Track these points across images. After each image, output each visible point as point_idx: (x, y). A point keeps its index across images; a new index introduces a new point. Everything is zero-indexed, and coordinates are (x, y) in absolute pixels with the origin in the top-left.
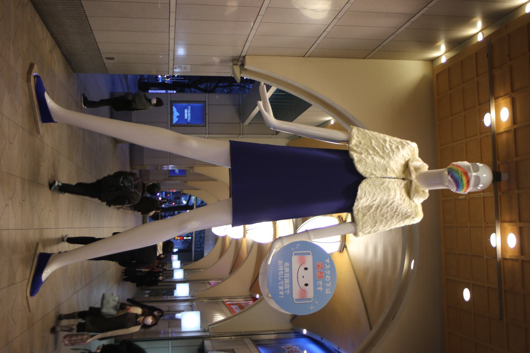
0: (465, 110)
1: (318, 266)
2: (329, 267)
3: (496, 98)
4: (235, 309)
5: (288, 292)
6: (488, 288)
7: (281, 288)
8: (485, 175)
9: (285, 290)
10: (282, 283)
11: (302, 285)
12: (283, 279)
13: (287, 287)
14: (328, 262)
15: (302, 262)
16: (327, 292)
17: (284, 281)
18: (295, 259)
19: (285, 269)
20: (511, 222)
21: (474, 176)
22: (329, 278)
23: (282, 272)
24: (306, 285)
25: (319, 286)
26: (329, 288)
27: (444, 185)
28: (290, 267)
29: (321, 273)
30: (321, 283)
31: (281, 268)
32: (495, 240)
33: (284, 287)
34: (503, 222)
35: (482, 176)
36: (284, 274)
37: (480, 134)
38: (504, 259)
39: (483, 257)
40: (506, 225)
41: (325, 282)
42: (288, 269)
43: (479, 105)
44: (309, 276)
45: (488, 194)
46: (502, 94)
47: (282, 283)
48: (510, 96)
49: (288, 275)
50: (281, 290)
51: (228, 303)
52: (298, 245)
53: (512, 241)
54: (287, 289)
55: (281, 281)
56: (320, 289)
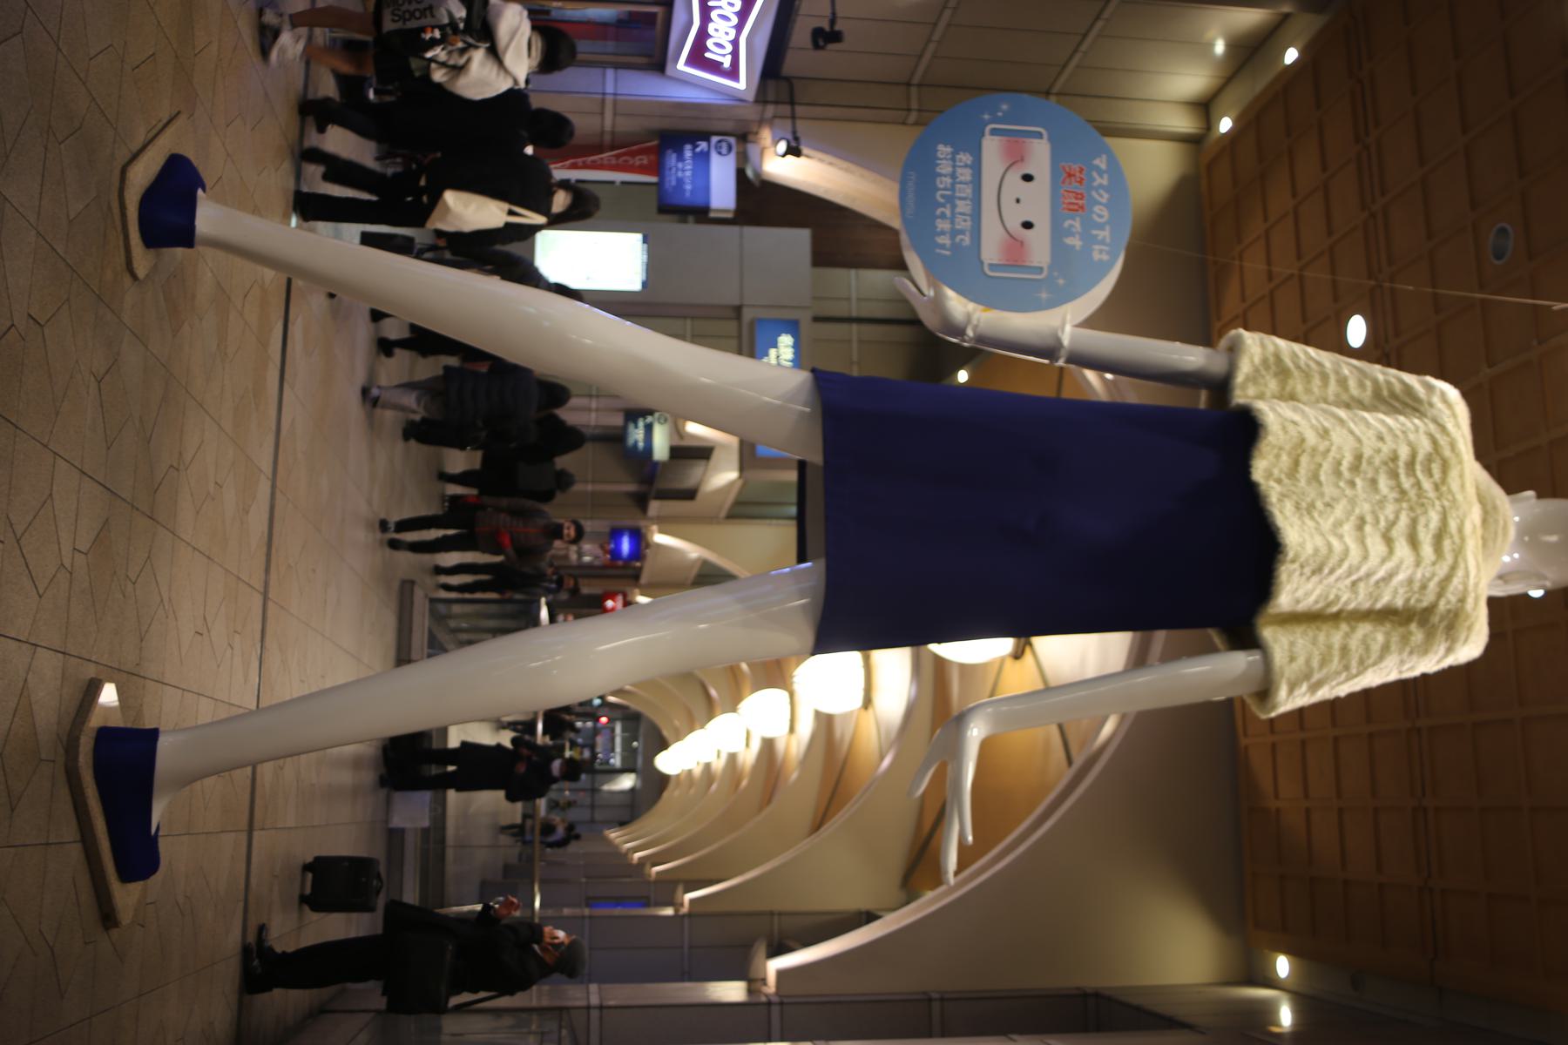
2: (1105, 182)
5: (967, 240)
7: (942, 225)
9: (954, 233)
10: (948, 212)
11: (1014, 225)
12: (951, 200)
13: (964, 224)
14: (1103, 166)
15: (1015, 157)
16: (1096, 256)
19: (959, 171)
22: (1105, 213)
23: (949, 180)
24: (1028, 225)
25: (1071, 234)
26: (1103, 242)
28: (977, 168)
29: (1079, 196)
30: (1077, 225)
31: (944, 168)
36: (953, 185)
41: (1089, 224)
44: (1037, 201)
47: (948, 212)
50: (943, 233)
54: (962, 232)
55: (943, 205)
56: (1075, 242)
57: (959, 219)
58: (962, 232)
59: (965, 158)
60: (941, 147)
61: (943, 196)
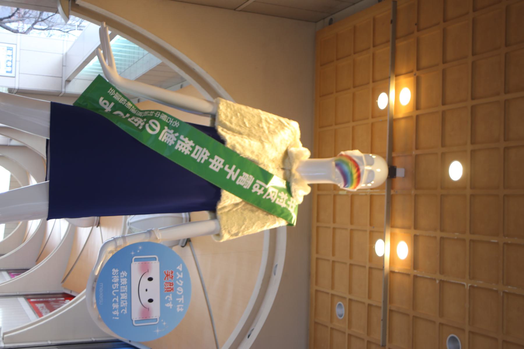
0: (354, 87)
3: (397, 76)
4: (40, 309)
6: (369, 305)
7: (115, 306)
8: (378, 170)
9: (120, 309)
11: (145, 301)
12: (118, 294)
13: (124, 304)
15: (145, 270)
17: (120, 297)
18: (135, 267)
19: (122, 280)
20: (402, 227)
21: (367, 170)
23: (117, 285)
27: (330, 179)
31: (116, 279)
32: (381, 248)
33: (119, 304)
34: (392, 227)
35: (375, 170)
36: (119, 287)
37: (373, 117)
38: (392, 272)
39: (365, 267)
40: (397, 231)
42: (125, 279)
43: (373, 82)
45: (376, 192)
46: (404, 71)
48: (415, 75)
49: (126, 288)
50: (115, 309)
51: (32, 300)
52: (140, 248)
53: (403, 250)
54: (124, 308)
55: (116, 297)
57: (122, 302)
58: (124, 308)
59: (124, 274)
60: (114, 270)
61: (115, 293)
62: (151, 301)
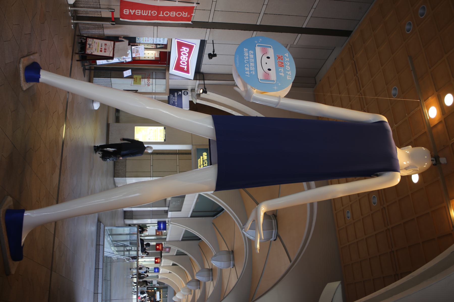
1: (279, 57)
7: (246, 69)
15: (265, 52)
31: (246, 54)
33: (249, 68)
36: (249, 58)
41: (285, 70)
50: (247, 71)
59: (251, 52)
62: (269, 70)
